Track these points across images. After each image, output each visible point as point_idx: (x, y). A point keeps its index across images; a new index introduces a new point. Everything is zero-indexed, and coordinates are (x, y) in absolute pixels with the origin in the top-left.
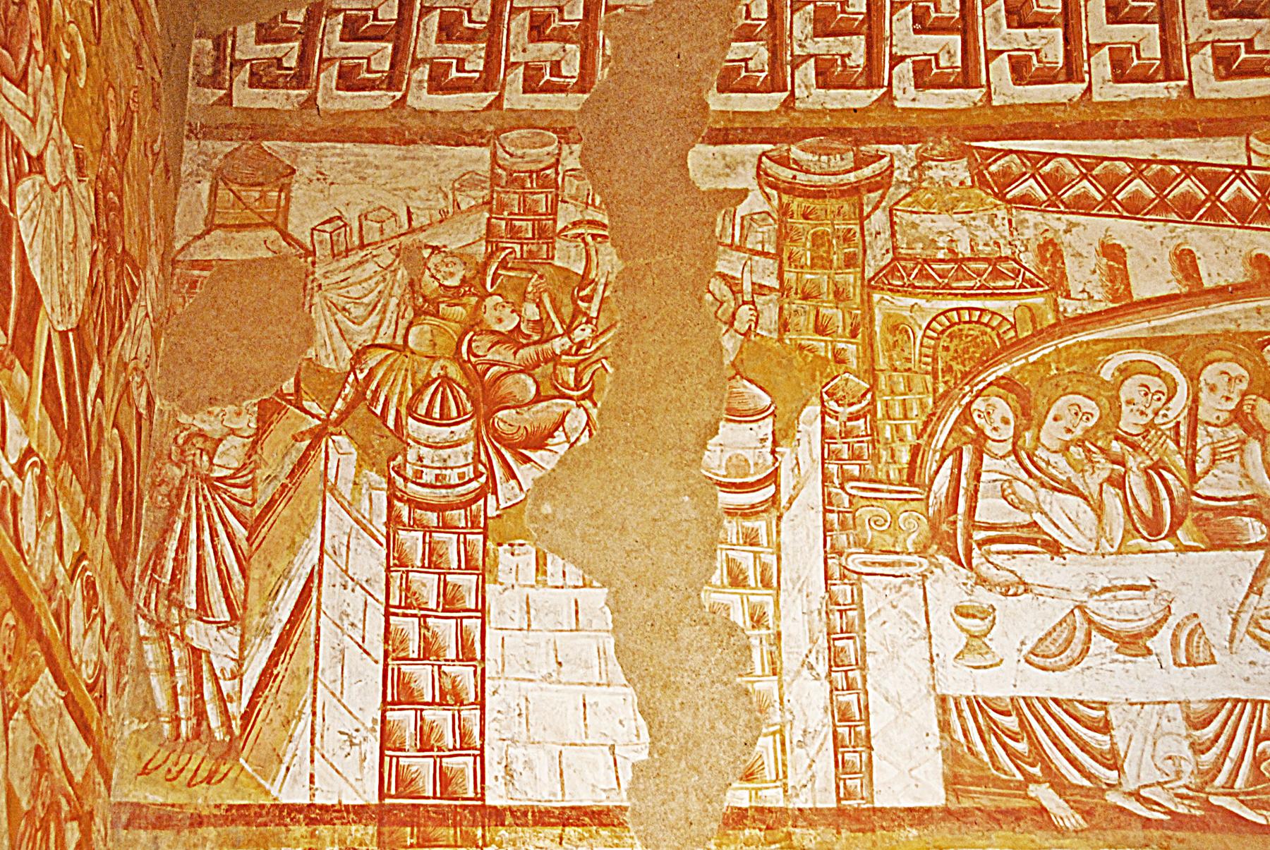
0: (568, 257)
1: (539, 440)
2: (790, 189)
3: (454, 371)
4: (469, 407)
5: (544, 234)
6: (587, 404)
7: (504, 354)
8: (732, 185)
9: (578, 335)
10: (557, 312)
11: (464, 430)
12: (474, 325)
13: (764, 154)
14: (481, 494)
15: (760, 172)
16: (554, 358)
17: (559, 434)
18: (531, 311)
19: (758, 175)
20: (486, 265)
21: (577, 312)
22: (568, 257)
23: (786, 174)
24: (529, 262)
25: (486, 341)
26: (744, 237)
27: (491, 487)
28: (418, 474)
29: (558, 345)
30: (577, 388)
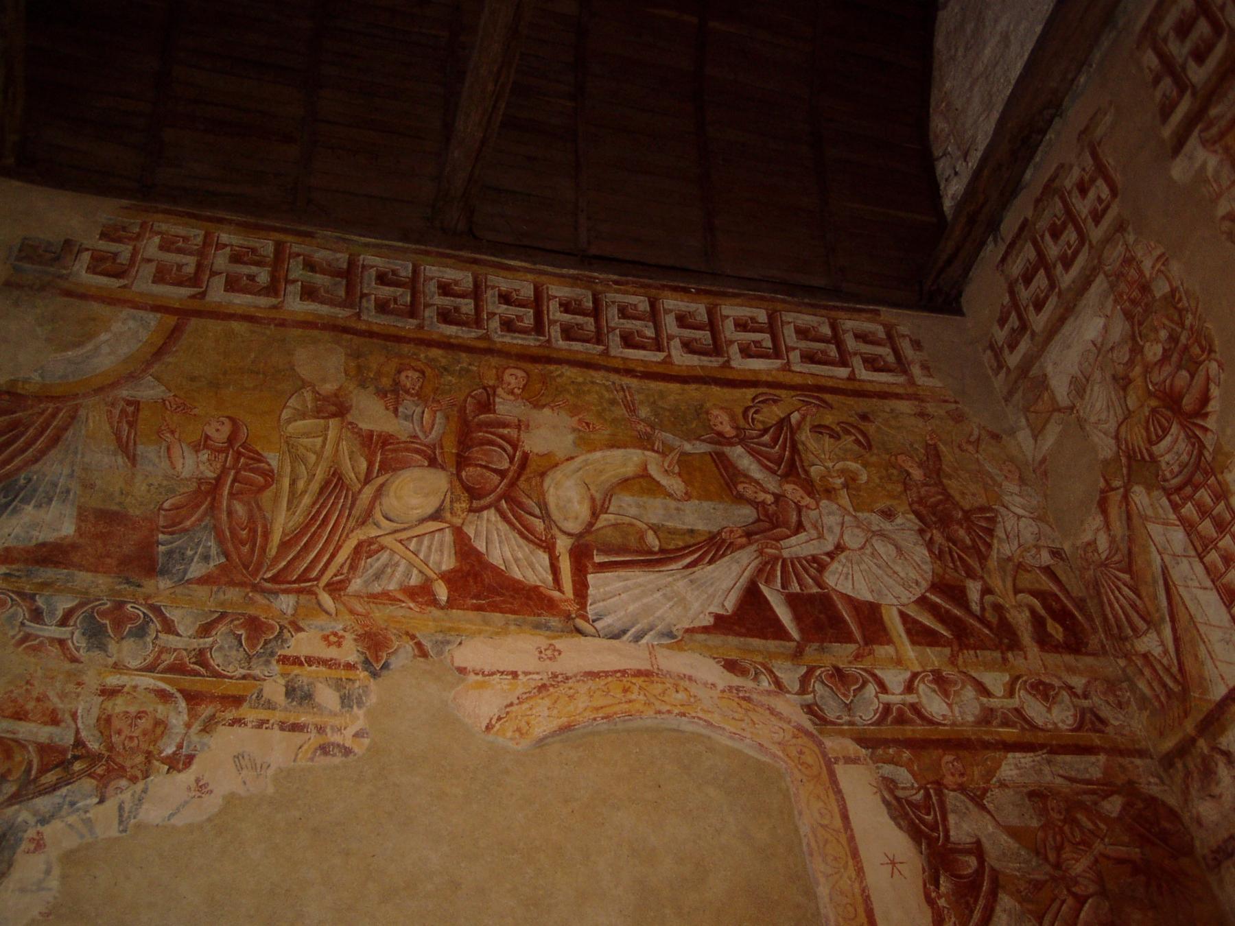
0: (1161, 289)
1: (1205, 399)
2: (1222, 135)
3: (1154, 403)
4: (1169, 413)
5: (1145, 288)
6: (1213, 355)
7: (1167, 369)
8: (1197, 165)
9: (1187, 323)
10: (1172, 320)
11: (1175, 429)
12: (1147, 370)
13: (1201, 131)
14: (1201, 454)
15: (1204, 143)
16: (1186, 348)
17: (1212, 386)
18: (1163, 334)
19: (1204, 146)
20: (1134, 333)
21: (1180, 311)
22: (1161, 289)
23: (1214, 131)
24: (1148, 310)
25: (1156, 371)
26: (1220, 185)
27: (1202, 446)
28: (1172, 472)
29: (1183, 340)
30: (1203, 351)
